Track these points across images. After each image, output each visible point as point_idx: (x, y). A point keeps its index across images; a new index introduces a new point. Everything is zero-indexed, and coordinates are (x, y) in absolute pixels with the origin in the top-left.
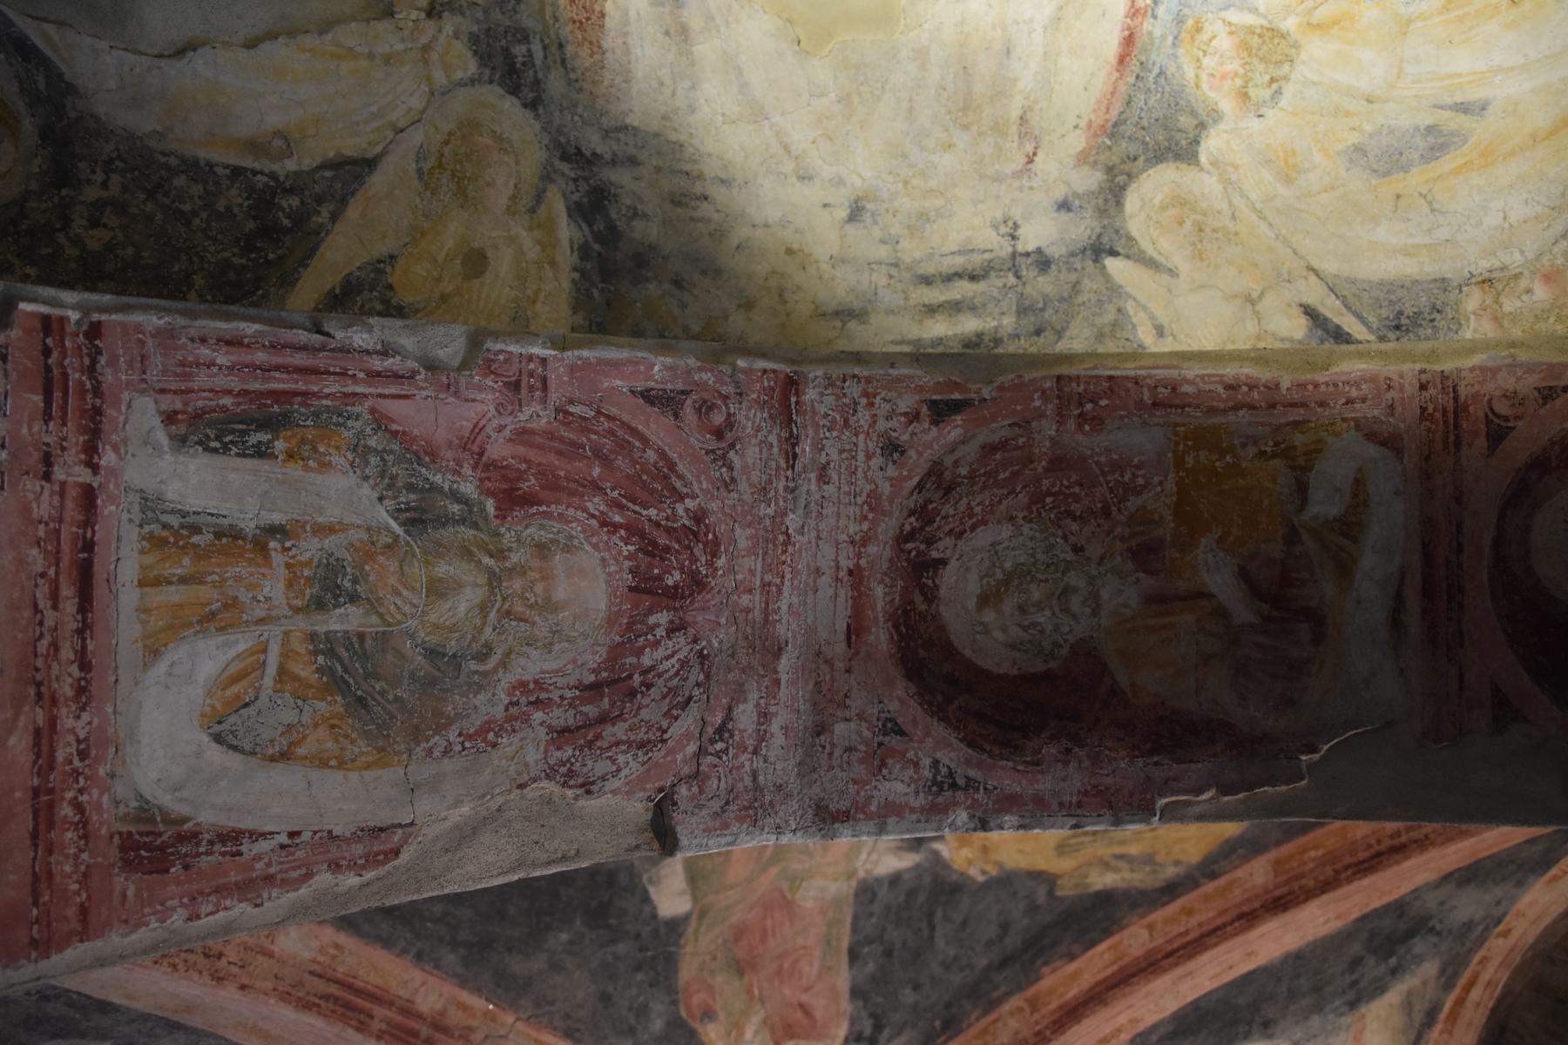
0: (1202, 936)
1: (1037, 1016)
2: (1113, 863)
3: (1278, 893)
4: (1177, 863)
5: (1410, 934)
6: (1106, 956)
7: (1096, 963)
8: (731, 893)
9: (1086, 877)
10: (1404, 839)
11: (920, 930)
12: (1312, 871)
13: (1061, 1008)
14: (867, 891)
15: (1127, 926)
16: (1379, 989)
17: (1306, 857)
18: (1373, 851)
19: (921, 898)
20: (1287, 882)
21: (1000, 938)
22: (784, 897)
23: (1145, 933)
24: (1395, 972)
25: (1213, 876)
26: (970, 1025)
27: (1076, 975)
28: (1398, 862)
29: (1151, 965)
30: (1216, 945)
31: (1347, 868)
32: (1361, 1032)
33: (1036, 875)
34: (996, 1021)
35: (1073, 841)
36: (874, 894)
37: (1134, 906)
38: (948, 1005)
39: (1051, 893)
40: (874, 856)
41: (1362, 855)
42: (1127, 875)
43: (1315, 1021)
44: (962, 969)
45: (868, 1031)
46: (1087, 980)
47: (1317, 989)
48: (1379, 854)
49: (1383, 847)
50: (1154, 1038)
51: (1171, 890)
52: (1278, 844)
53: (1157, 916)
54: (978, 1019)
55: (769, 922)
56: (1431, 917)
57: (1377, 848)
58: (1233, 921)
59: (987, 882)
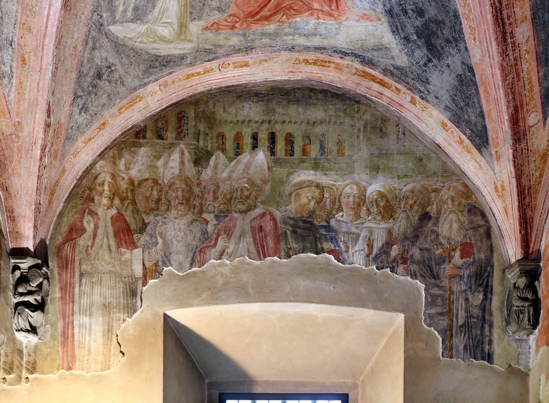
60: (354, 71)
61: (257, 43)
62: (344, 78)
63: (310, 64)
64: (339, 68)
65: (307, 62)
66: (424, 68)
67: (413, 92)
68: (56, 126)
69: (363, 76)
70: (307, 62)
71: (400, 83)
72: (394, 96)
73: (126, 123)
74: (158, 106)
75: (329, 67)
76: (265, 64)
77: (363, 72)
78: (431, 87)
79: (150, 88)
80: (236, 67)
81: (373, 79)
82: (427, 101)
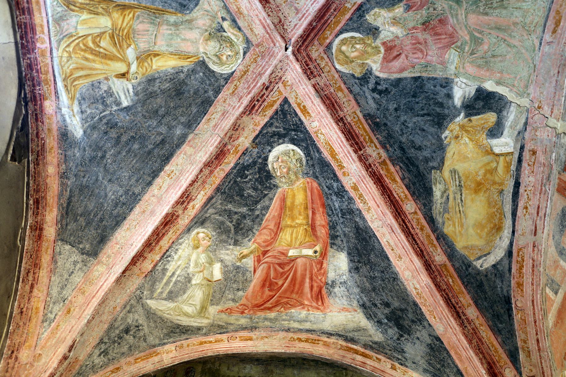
0: (412, 235)
1: (377, 165)
2: (445, 195)
3: (433, 266)
4: (444, 223)
5: (400, 327)
6: (402, 194)
7: (399, 189)
8: (464, 16)
9: (440, 183)
10: (463, 317)
11: (423, 110)
12: (443, 280)
13: (381, 175)
14: (447, 84)
15: (416, 203)
16: (369, 317)
17: (449, 277)
18: (456, 305)
19: (438, 110)
20: (438, 270)
21: (414, 147)
22: (453, 44)
23: (413, 211)
24: (379, 322)
25: (438, 239)
26: (375, 135)
27: (394, 180)
28: (453, 316)
29: (399, 214)
30: (409, 241)
31: (447, 294)
32: (347, 310)
33: (442, 162)
34: (376, 147)
35: (457, 177)
36: (444, 87)
37: (425, 205)
38: (385, 125)
39: (434, 168)
40: (463, 86)
41: (453, 300)
42: (439, 202)
43: (357, 290)
44: (401, 130)
45: (379, 87)
46: (392, 186)
47: (374, 289)
48: (455, 307)
49: (458, 309)
50: (358, 220)
51: (431, 221)
52: (453, 266)
53: (420, 216)
54: (377, 138)
55: (444, 37)
56: (409, 335)
57: (457, 306)
58: (419, 248)
59: (441, 139)
60: (339, 347)
61: (261, 324)
62: (331, 351)
63: (303, 341)
64: (326, 344)
65: (300, 340)
66: (398, 342)
67: (392, 360)
68: (72, 361)
69: (348, 350)
70: (300, 340)
71: (380, 354)
72: (376, 365)
73: (138, 371)
74: (170, 362)
75: (318, 344)
76: (266, 340)
77: (347, 347)
78: (406, 355)
79: (167, 347)
80: (242, 340)
81: (356, 352)
82: (407, 367)
